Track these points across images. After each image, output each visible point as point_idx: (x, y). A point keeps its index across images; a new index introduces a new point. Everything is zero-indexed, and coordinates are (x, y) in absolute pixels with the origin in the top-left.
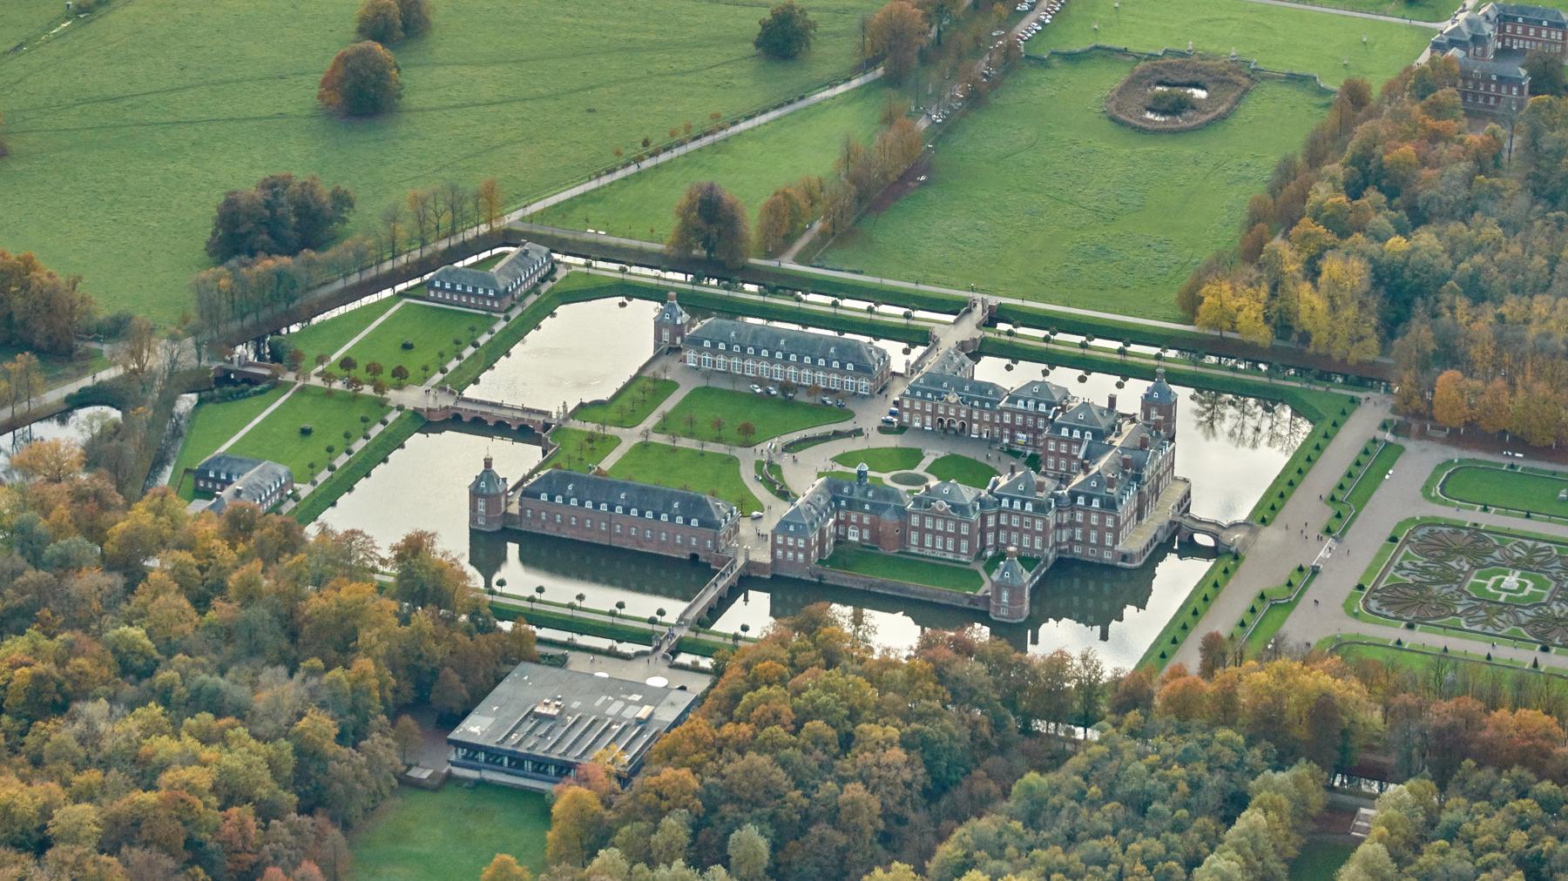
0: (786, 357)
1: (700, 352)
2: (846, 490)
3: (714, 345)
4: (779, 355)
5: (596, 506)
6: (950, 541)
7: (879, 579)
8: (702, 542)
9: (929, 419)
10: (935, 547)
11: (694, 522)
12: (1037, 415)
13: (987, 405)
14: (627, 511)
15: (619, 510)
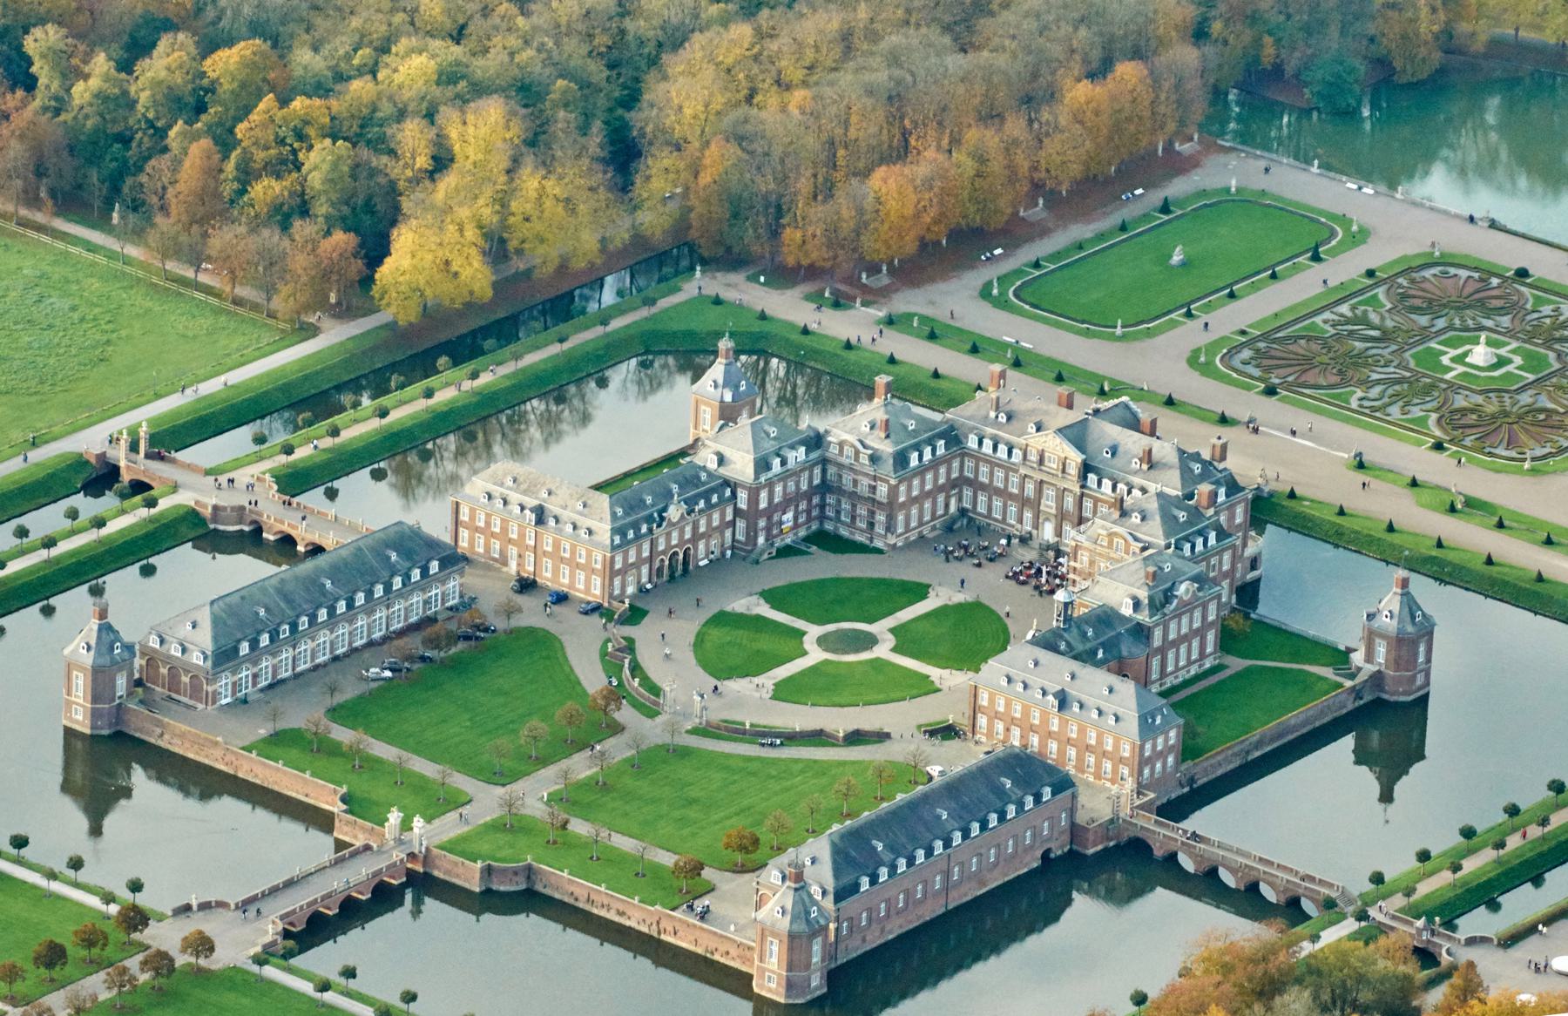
0: (350, 605)
1: (234, 673)
2: (1063, 646)
3: (254, 644)
4: (341, 607)
5: (929, 852)
6: (1195, 644)
7: (1255, 735)
8: (1054, 821)
9: (645, 570)
10: (1182, 663)
11: (1047, 792)
12: (796, 474)
13: (715, 499)
14: (966, 834)
15: (957, 837)
